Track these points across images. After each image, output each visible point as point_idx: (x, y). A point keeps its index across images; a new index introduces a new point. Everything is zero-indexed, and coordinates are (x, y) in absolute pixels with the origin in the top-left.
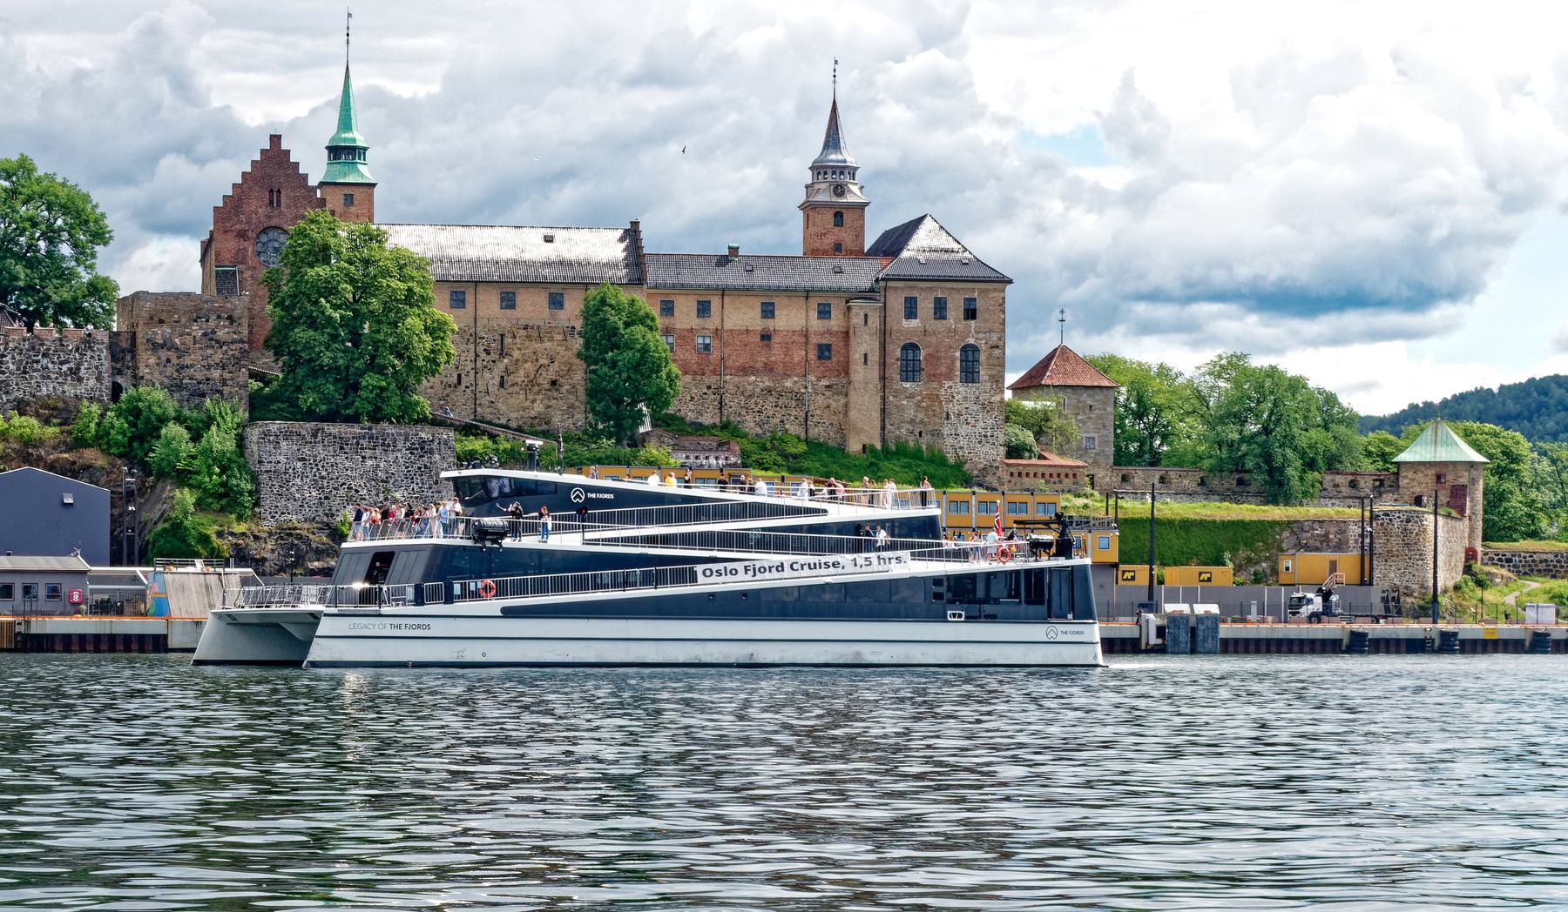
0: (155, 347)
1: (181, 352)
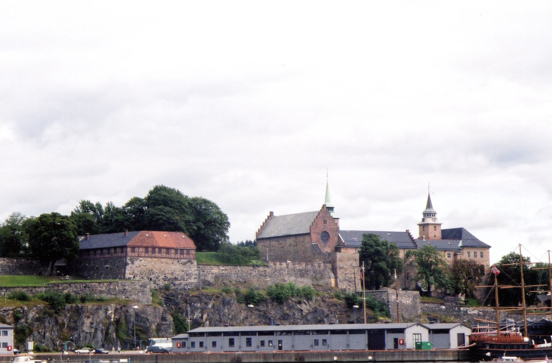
0: (341, 268)
1: (346, 270)
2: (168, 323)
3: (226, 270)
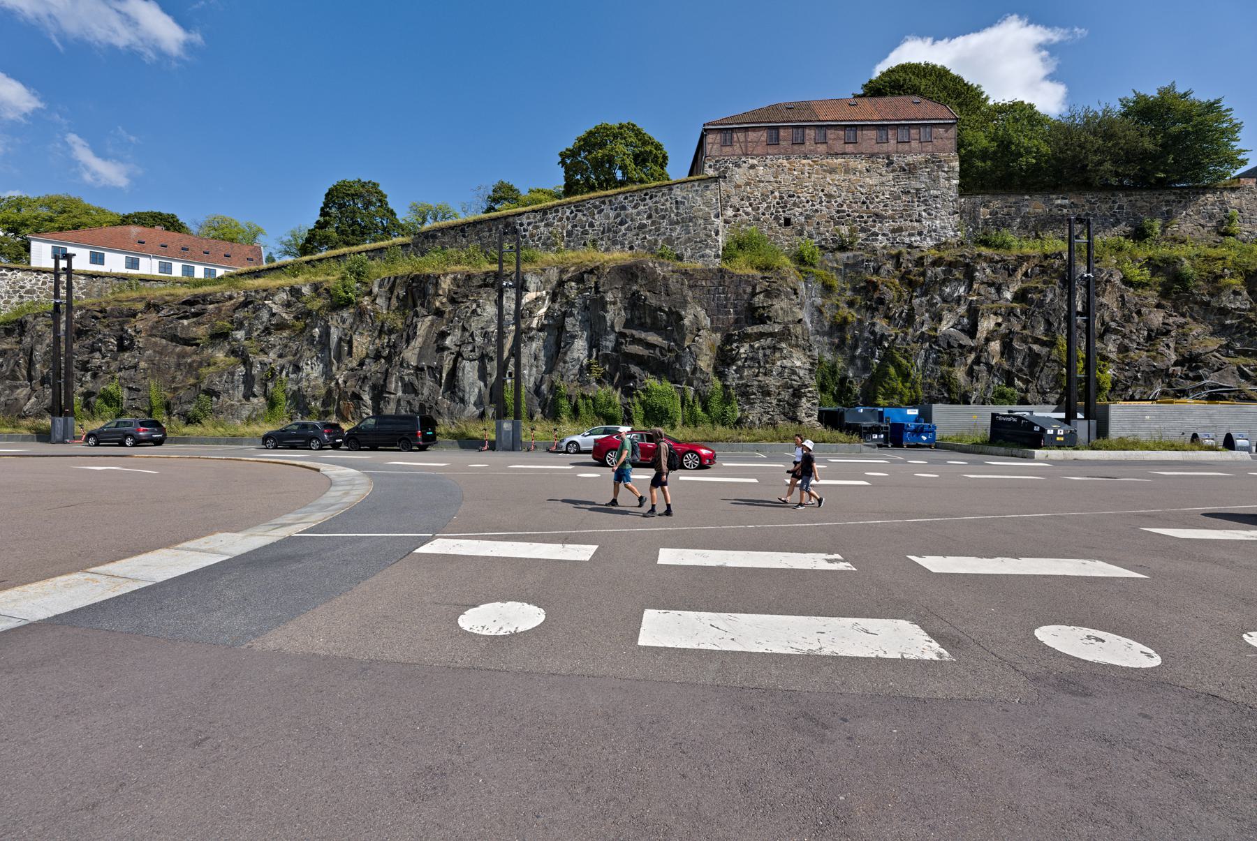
2: (777, 328)
3: (1073, 205)
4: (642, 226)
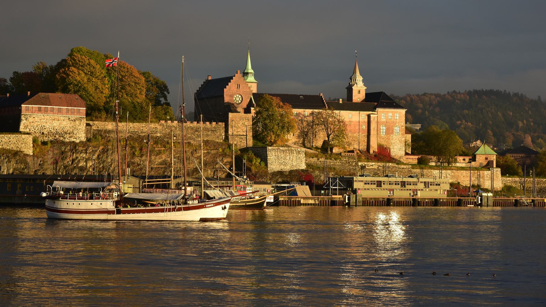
4: (14, 143)
